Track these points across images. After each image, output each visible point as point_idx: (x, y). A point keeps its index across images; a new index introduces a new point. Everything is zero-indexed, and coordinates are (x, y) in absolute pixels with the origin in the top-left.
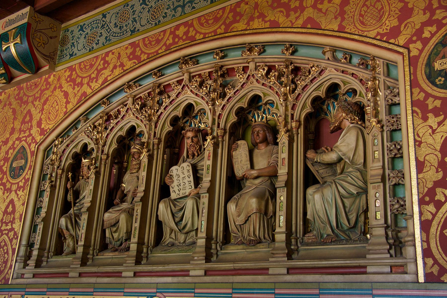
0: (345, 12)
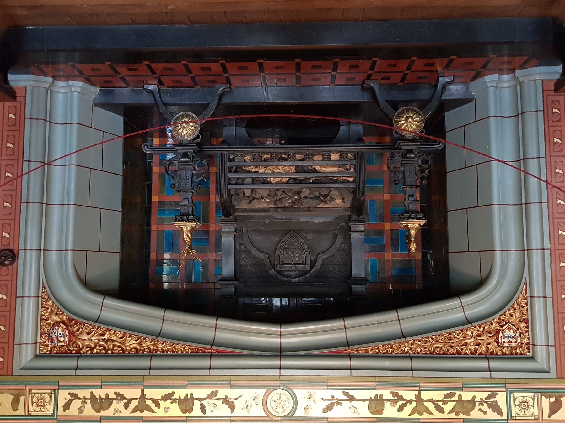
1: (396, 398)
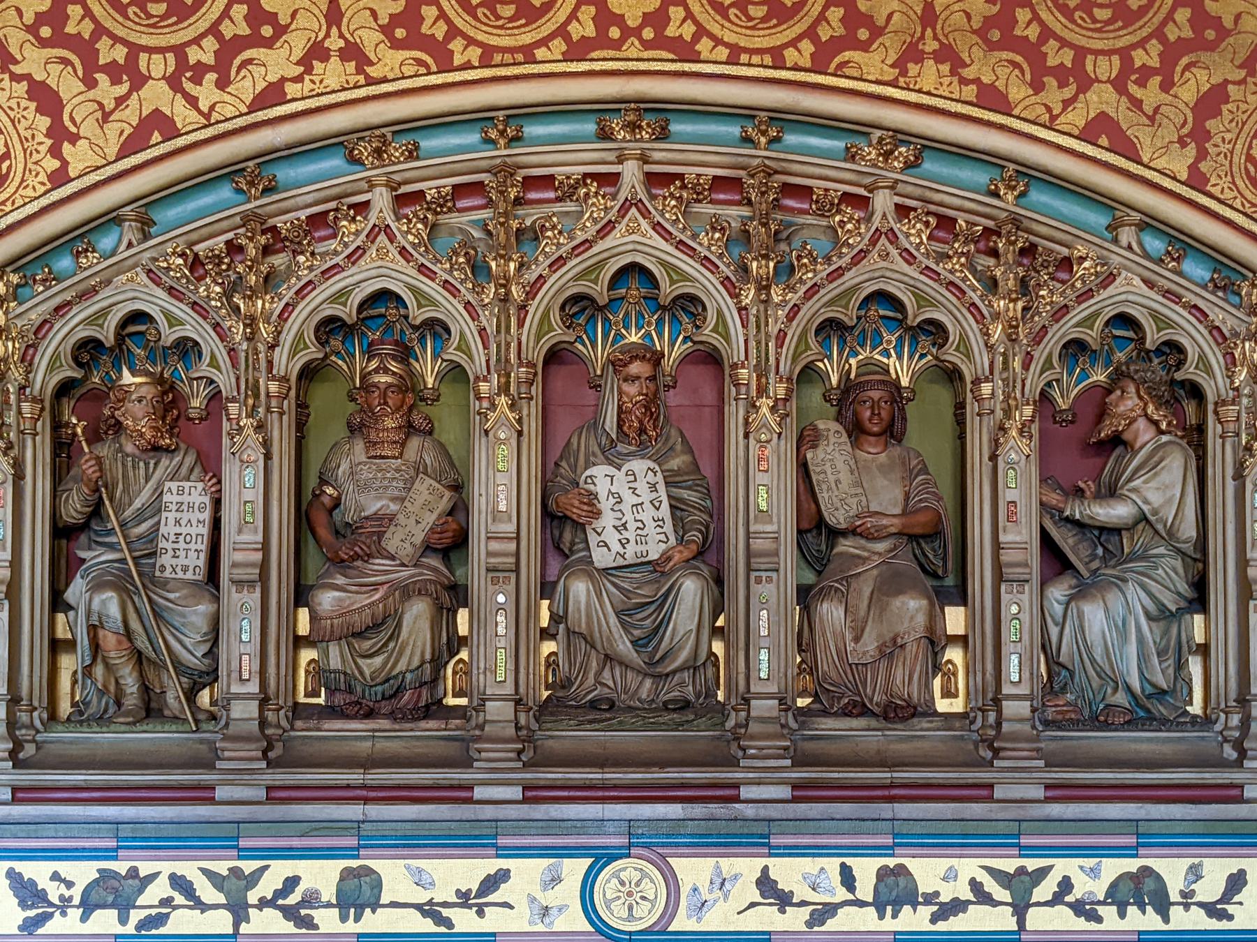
0: (1208, 135)
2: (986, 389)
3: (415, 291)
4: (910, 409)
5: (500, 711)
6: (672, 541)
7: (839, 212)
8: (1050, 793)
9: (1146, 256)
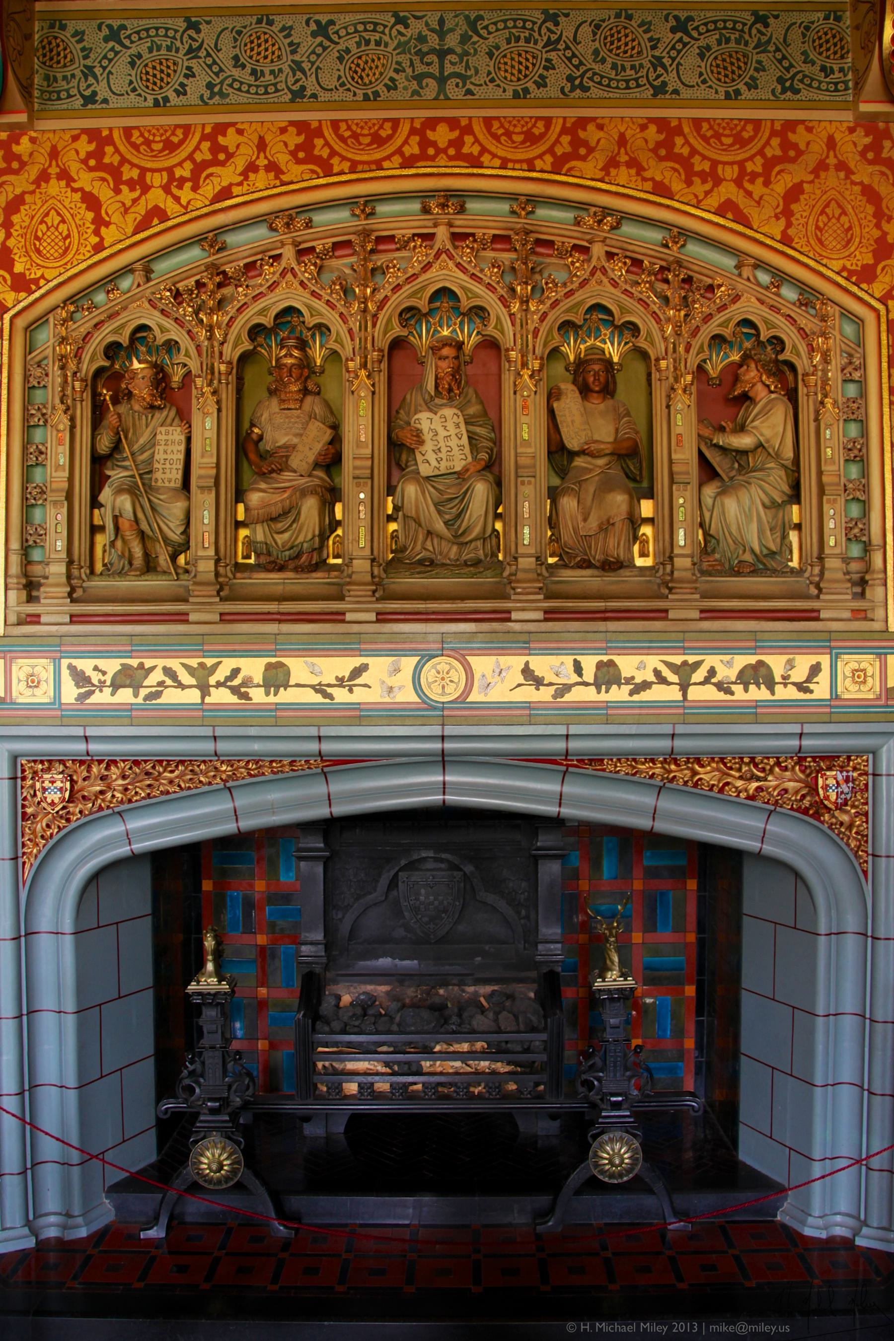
1: (243, 690)
2: (663, 364)
3: (309, 307)
4: (619, 377)
5: (361, 566)
6: (470, 459)
7: (571, 256)
8: (703, 615)
9: (759, 284)
